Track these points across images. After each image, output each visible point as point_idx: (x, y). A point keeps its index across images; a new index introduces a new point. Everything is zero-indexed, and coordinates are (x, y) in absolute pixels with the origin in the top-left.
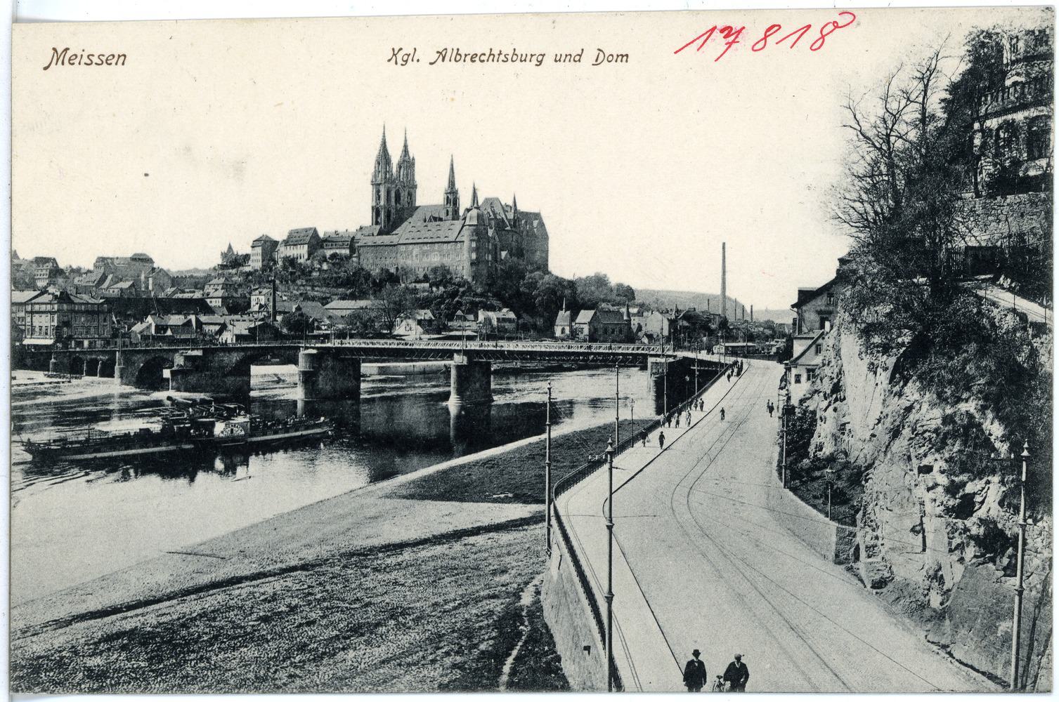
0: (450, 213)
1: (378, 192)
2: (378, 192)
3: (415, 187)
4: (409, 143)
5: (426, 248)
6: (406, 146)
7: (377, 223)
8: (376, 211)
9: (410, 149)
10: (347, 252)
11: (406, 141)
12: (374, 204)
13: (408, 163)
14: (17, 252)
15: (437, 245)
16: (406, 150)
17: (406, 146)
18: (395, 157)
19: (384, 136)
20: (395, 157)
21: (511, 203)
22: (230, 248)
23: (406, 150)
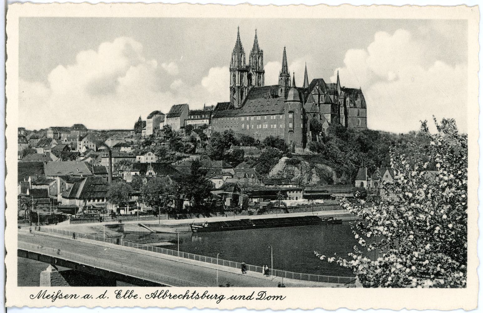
0: (283, 91)
1: (234, 76)
2: (234, 76)
5: (259, 118)
7: (232, 98)
8: (233, 90)
10: (208, 120)
11: (256, 37)
12: (232, 86)
13: (257, 53)
15: (266, 117)
16: (256, 42)
18: (248, 49)
19: (238, 35)
20: (248, 49)
21: (336, 83)
22: (140, 118)
23: (256, 42)
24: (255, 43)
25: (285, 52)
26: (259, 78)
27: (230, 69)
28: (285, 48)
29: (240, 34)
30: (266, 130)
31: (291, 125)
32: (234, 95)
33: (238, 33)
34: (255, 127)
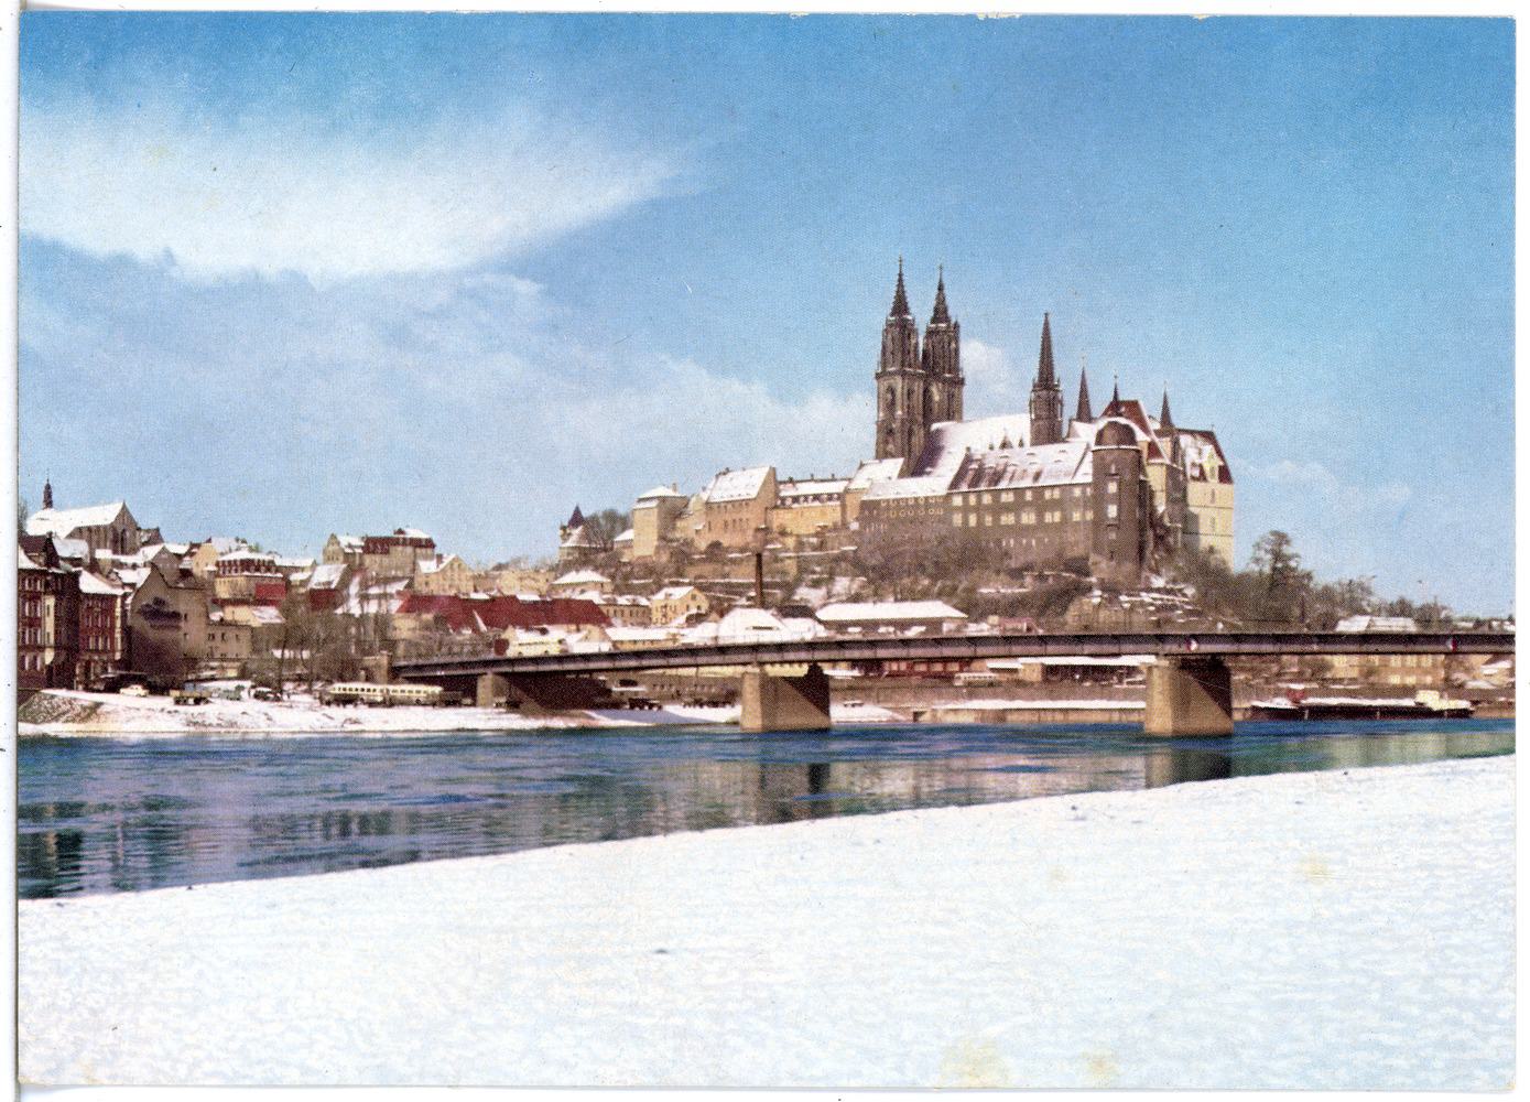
3: (961, 382)
4: (946, 291)
6: (941, 299)
9: (949, 302)
13: (945, 333)
14: (161, 531)
17: (941, 299)
18: (921, 315)
19: (900, 280)
20: (921, 315)
24: (938, 303)
25: (1046, 324)
26: (951, 397)
27: (877, 374)
28: (1046, 314)
29: (904, 278)
30: (1028, 528)
31: (1112, 511)
32: (887, 442)
33: (900, 275)
34: (996, 520)
